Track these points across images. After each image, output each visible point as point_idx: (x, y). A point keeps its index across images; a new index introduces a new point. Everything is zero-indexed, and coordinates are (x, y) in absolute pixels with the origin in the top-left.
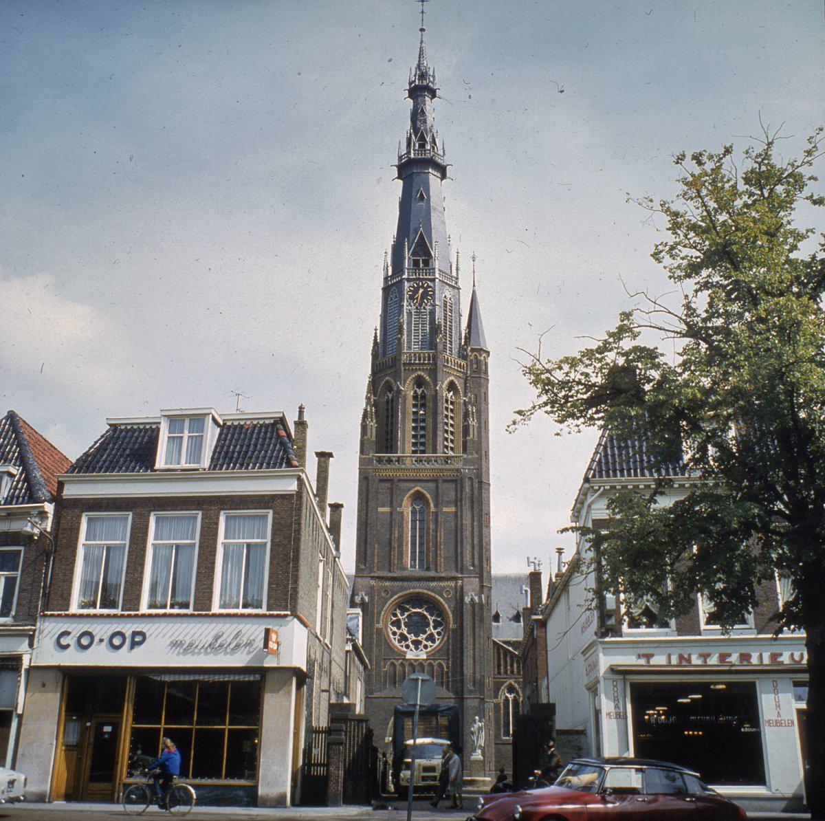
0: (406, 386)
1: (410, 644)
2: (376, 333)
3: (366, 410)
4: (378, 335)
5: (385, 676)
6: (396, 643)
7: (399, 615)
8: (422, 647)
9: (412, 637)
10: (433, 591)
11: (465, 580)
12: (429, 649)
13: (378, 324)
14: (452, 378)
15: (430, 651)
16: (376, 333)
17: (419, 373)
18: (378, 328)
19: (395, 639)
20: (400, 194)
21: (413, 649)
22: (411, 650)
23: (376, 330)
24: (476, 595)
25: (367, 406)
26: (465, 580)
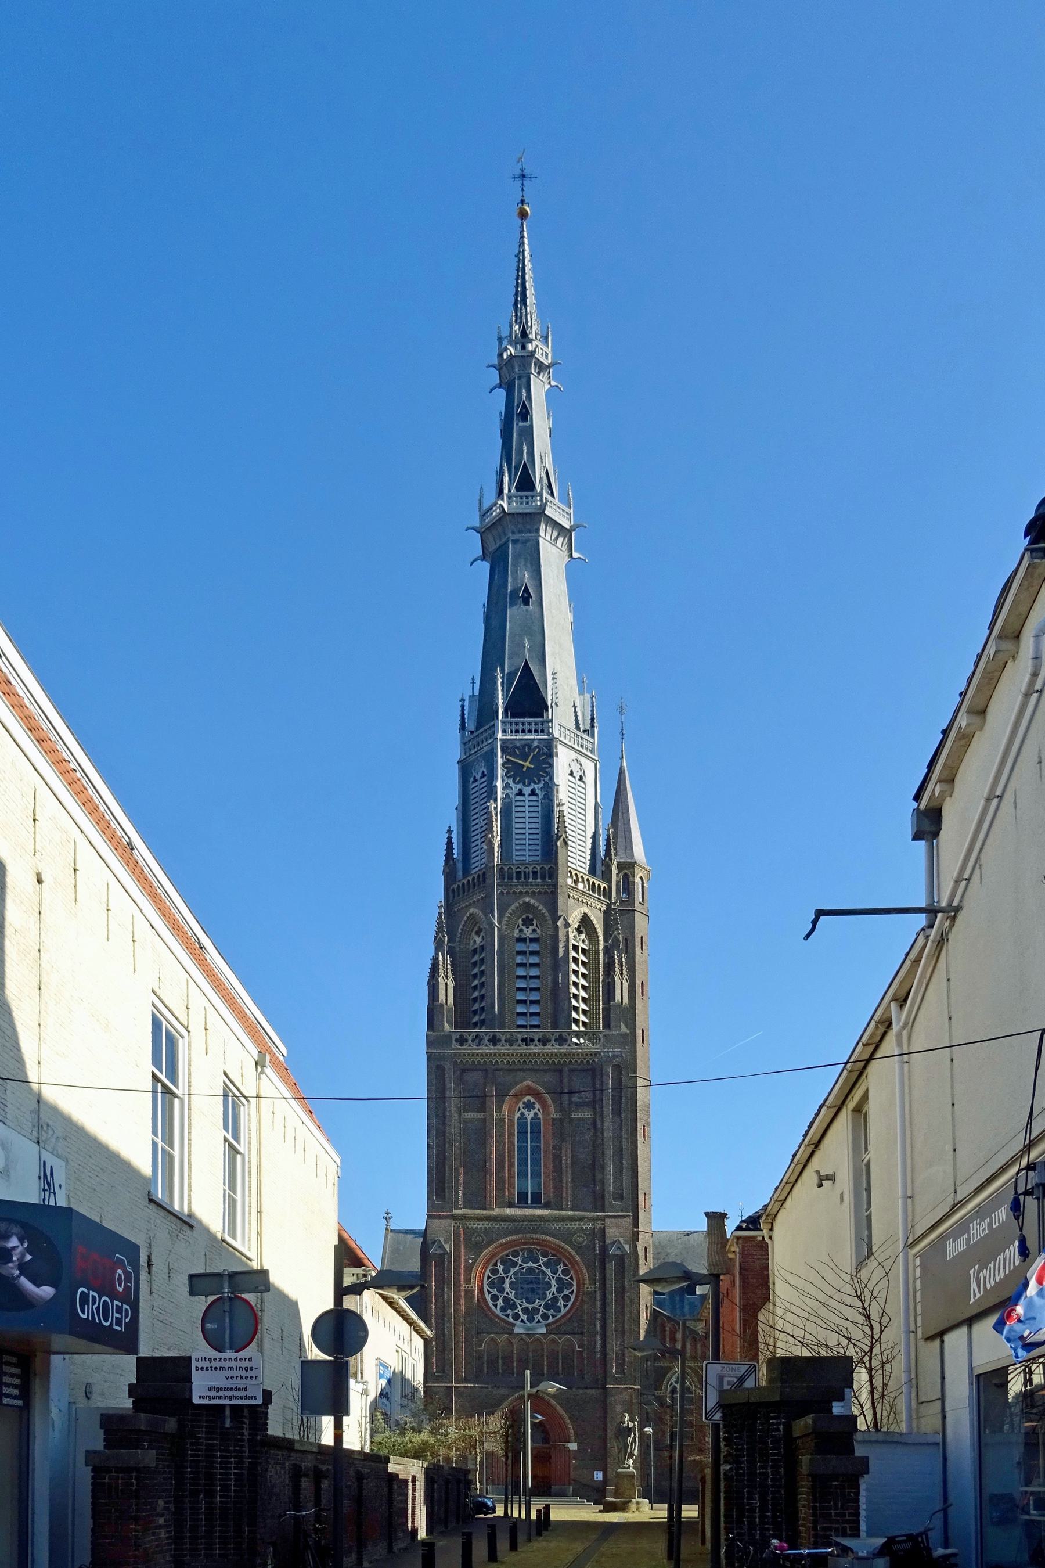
0: (504, 922)
1: (520, 1313)
2: (450, 839)
3: (435, 960)
4: (454, 840)
5: (480, 1358)
6: (498, 1311)
7: (501, 1271)
8: (540, 1318)
9: (521, 1304)
10: (554, 1236)
11: (607, 1220)
12: (551, 1320)
13: (452, 820)
14: (586, 910)
15: (553, 1323)
16: (450, 839)
17: (527, 899)
18: (454, 828)
19: (496, 1306)
20: (485, 599)
21: (525, 1320)
22: (522, 1321)
23: (449, 831)
24: (626, 1242)
25: (437, 954)
26: (607, 1220)
